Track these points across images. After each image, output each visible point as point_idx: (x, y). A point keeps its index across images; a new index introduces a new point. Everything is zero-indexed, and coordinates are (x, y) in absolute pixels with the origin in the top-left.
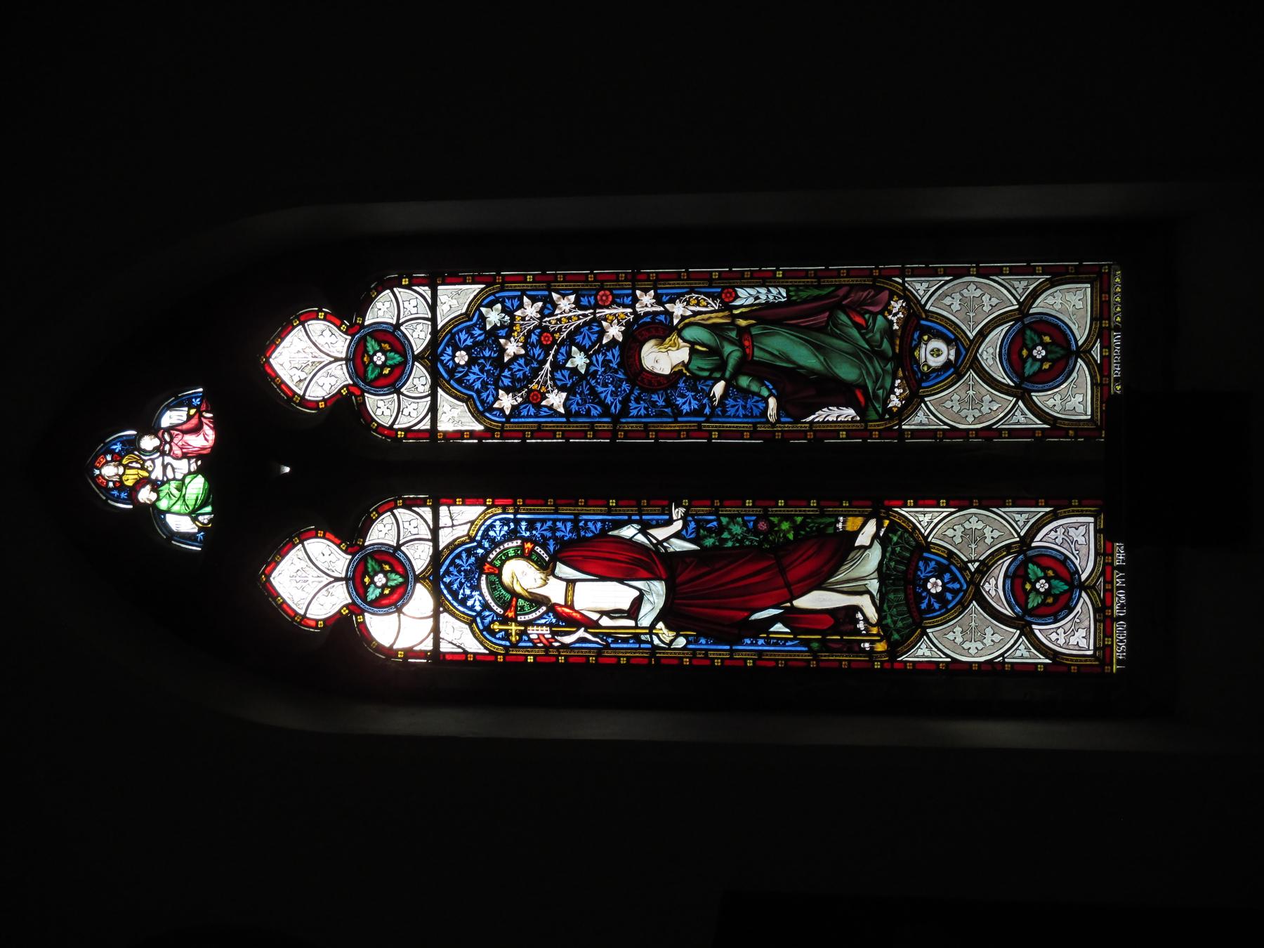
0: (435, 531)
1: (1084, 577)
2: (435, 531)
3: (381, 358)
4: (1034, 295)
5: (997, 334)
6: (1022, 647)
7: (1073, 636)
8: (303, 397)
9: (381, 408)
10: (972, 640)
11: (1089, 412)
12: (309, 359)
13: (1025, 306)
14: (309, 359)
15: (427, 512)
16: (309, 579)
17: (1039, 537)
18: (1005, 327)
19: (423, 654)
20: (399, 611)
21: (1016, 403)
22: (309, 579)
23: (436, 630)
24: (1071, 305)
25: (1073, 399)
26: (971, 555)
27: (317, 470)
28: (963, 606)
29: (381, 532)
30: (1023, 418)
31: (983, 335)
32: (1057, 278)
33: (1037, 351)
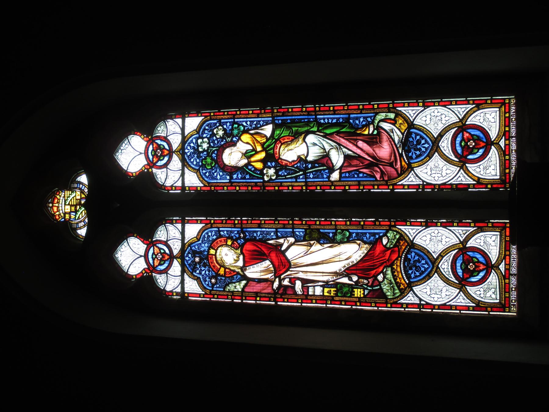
0: (183, 233)
1: (493, 263)
2: (183, 233)
3: (159, 153)
4: (468, 115)
5: (449, 135)
6: (461, 297)
7: (488, 291)
8: (126, 171)
9: (160, 175)
10: (436, 293)
11: (498, 174)
12: (132, 155)
13: (463, 120)
14: (132, 155)
15: (179, 226)
16: (131, 256)
17: (469, 243)
18: (453, 131)
19: (177, 294)
20: (167, 273)
21: (459, 171)
22: (131, 256)
23: (182, 282)
24: (489, 119)
25: (489, 168)
26: (435, 249)
27: (136, 206)
28: (429, 277)
29: (161, 234)
30: (463, 179)
31: (441, 135)
32: (479, 106)
33: (470, 144)
